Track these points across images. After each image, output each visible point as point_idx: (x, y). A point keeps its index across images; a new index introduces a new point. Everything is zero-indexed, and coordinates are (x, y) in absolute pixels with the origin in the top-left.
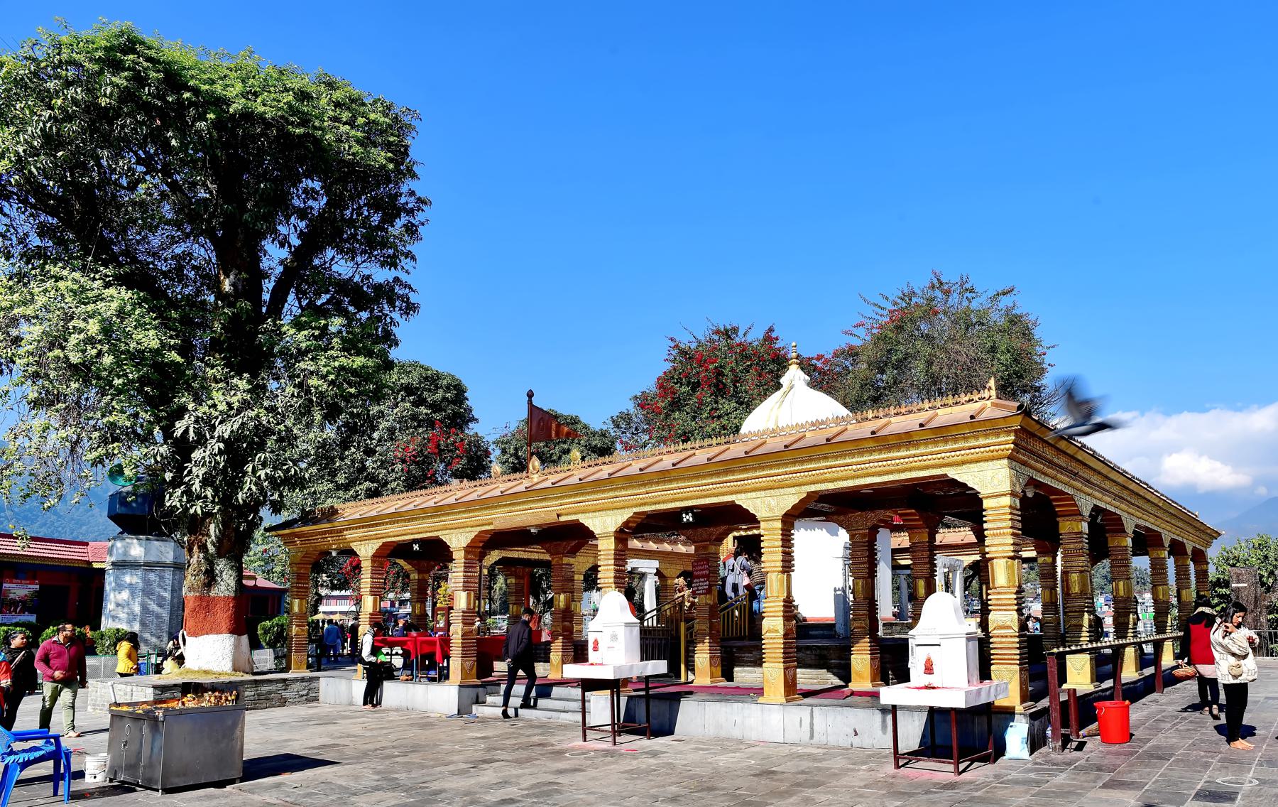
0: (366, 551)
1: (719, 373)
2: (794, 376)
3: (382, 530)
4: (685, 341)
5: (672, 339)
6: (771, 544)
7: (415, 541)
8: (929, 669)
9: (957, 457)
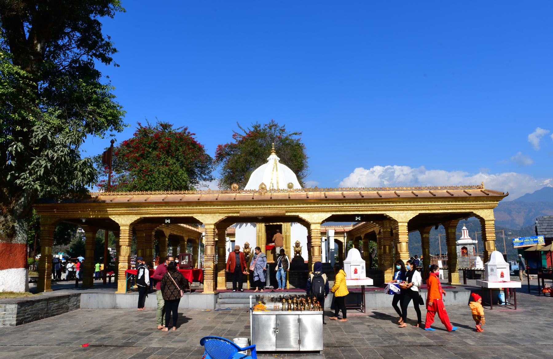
0: (124, 221)
1: (169, 145)
2: (273, 158)
3: (143, 210)
4: (144, 125)
5: (139, 124)
6: (403, 231)
8: (502, 276)
9: (478, 206)
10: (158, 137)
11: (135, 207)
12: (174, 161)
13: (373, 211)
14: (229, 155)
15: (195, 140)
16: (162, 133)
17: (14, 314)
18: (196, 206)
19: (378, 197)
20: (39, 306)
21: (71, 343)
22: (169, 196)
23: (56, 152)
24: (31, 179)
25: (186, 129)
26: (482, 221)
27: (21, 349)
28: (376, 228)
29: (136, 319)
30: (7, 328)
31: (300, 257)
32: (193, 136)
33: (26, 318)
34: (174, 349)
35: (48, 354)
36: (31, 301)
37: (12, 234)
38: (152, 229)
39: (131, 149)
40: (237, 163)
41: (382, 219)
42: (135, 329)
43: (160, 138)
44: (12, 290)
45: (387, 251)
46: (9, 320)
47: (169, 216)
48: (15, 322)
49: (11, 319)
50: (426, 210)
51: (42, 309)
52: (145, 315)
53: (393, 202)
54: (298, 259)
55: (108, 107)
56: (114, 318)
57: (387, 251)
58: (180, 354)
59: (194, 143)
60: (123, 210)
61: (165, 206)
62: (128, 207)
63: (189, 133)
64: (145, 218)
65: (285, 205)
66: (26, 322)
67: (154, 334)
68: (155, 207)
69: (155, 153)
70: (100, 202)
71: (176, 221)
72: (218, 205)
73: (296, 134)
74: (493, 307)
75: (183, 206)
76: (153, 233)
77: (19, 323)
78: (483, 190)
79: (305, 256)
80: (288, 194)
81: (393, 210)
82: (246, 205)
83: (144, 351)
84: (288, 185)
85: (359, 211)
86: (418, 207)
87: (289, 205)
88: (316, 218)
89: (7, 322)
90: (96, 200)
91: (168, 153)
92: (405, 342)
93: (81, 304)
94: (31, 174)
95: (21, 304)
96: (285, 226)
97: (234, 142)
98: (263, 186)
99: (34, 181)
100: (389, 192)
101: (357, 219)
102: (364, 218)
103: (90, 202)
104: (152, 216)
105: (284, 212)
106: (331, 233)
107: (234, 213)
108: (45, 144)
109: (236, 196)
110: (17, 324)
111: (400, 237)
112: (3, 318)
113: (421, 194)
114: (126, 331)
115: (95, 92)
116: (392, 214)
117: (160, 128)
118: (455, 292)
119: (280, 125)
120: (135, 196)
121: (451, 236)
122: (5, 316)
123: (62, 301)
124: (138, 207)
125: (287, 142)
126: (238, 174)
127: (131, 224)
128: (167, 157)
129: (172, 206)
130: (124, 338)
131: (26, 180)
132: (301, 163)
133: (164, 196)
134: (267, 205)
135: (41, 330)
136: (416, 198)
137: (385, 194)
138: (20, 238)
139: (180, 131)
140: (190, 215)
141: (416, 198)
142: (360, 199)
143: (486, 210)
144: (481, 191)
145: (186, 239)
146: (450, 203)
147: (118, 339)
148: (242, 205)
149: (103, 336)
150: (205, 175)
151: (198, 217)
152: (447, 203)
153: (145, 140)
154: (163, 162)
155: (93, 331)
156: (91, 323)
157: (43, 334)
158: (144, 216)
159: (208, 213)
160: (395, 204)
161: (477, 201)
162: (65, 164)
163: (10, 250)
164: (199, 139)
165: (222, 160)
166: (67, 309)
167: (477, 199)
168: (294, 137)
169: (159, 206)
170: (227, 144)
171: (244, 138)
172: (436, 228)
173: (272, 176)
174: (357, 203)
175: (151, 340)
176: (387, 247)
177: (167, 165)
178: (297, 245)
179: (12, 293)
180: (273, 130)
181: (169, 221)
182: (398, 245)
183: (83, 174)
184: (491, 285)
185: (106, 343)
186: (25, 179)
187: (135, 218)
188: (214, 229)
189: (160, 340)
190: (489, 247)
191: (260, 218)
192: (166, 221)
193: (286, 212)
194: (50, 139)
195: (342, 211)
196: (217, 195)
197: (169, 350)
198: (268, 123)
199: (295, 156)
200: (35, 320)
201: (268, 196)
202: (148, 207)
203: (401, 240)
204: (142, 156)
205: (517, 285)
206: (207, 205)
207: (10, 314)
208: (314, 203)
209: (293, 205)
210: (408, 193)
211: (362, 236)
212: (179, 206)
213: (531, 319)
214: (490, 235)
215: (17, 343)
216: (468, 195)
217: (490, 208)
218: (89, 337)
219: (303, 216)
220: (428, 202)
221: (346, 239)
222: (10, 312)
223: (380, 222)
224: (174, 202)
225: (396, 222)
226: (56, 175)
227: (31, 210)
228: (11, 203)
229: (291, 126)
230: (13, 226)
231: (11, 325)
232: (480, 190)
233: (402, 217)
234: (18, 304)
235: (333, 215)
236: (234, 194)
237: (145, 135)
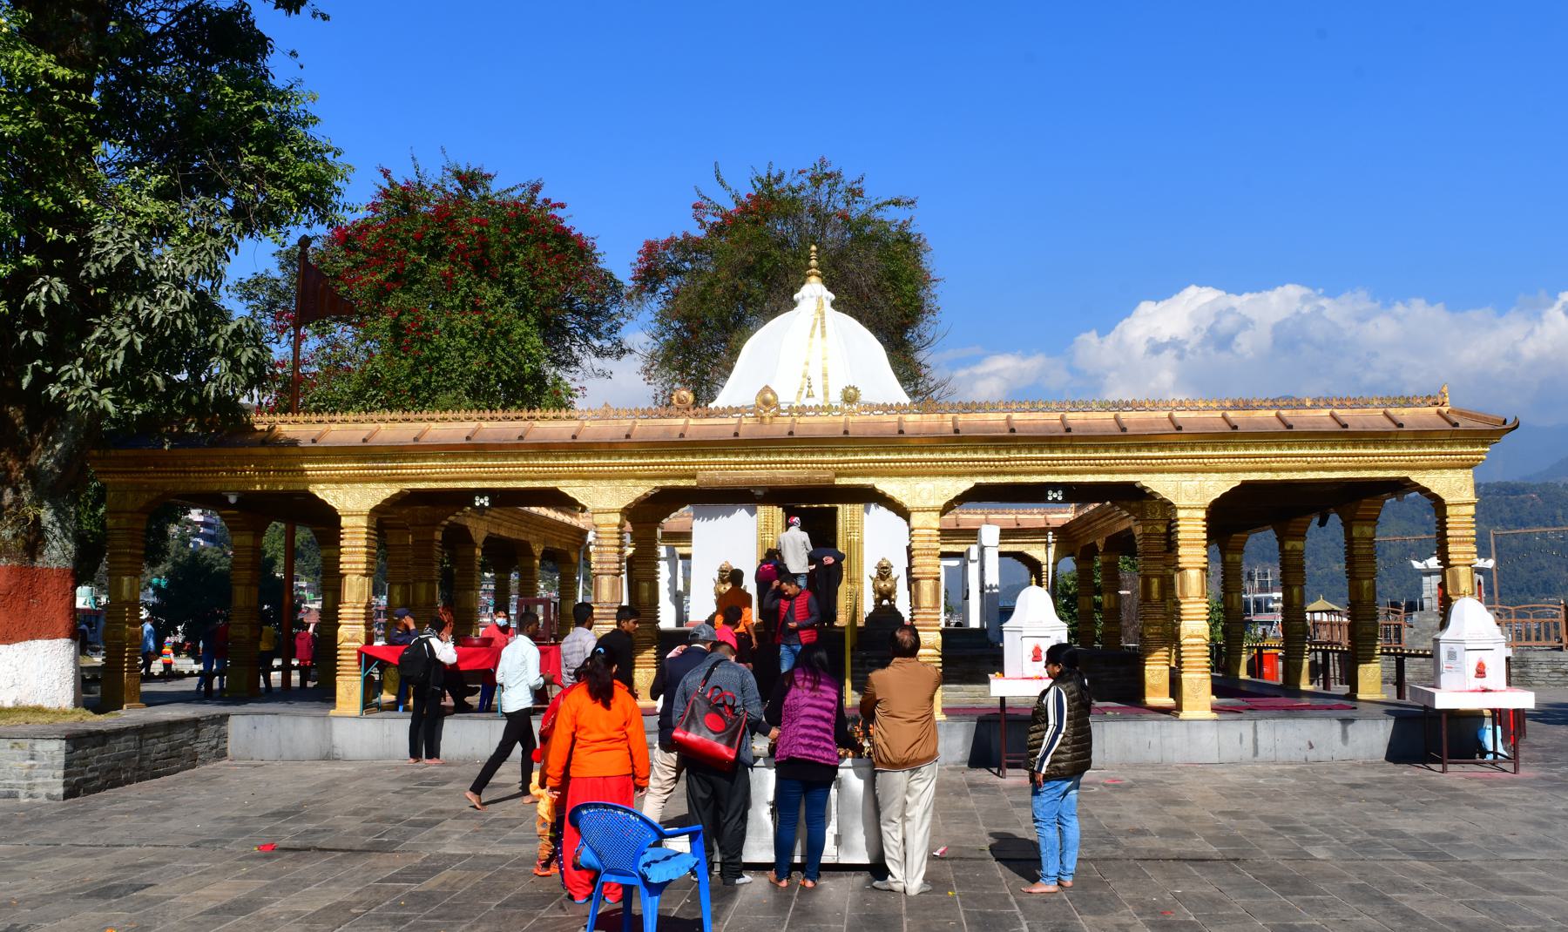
0: (354, 501)
2: (814, 293)
3: (410, 468)
5: (386, 174)
7: (482, 492)
8: (1481, 672)
10: (444, 217)
11: (384, 459)
12: (499, 292)
13: (1099, 472)
14: (677, 272)
15: (566, 225)
16: (460, 200)
17: (58, 767)
18: (567, 457)
19: (1116, 431)
20: (120, 746)
21: (228, 842)
22: (484, 424)
23: (158, 303)
24: (89, 383)
25: (536, 188)
26: (1438, 504)
27: (100, 853)
28: (1126, 522)
29: (397, 787)
30: (41, 805)
31: (892, 609)
32: (559, 212)
33: (87, 781)
34: (504, 859)
35: (177, 865)
36: (99, 733)
37: (34, 541)
38: (433, 523)
39: (361, 256)
40: (703, 300)
41: (1132, 495)
42: (394, 811)
43: (452, 221)
44: (39, 702)
45: (1155, 595)
46: (45, 784)
47: (486, 485)
48: (60, 791)
49: (50, 780)
50: (1263, 470)
51: (129, 757)
52: (419, 776)
53: (1162, 447)
54: (885, 615)
55: (299, 154)
56: (331, 785)
57: (1155, 595)
58: (522, 869)
59: (563, 235)
60: (348, 468)
61: (475, 457)
62: (365, 460)
63: (546, 201)
64: (416, 494)
65: (834, 453)
66: (89, 792)
67: (448, 824)
68: (445, 458)
69: (438, 269)
70: (282, 445)
71: (507, 499)
72: (631, 455)
73: (897, 203)
74: (1450, 767)
75: (526, 456)
76: (438, 536)
77: (71, 792)
78: (1445, 410)
79: (903, 605)
80: (842, 419)
81: (1162, 472)
82: (715, 454)
83: (424, 861)
84: (845, 391)
85: (1058, 473)
86: (1239, 463)
87: (845, 453)
88: (927, 492)
89: (38, 790)
90: (270, 440)
91: (482, 266)
92: (1137, 851)
93: (232, 746)
94: (87, 366)
95: (77, 741)
96: (845, 512)
97: (698, 233)
98: (769, 396)
99: (98, 390)
100: (1153, 415)
101: (1051, 495)
102: (1075, 493)
103: (253, 444)
104: (434, 485)
105: (829, 475)
106: (990, 535)
107: (681, 477)
108: (128, 279)
109: (686, 426)
110: (66, 796)
111: (1181, 551)
112: (28, 777)
113: (1249, 421)
114: (372, 815)
115: (260, 113)
116: (1159, 484)
117: (453, 186)
118: (1346, 721)
119: (849, 177)
120: (383, 425)
121: (1361, 549)
122: (34, 773)
123: (179, 737)
124: (393, 459)
125: (868, 230)
126: (701, 347)
127: (375, 511)
128: (480, 284)
129: (495, 457)
130: (367, 832)
131: (79, 387)
132: (917, 298)
133: (472, 425)
134: (780, 453)
135: (136, 812)
136: (1231, 436)
137: (1138, 423)
138: (57, 553)
139: (516, 194)
140: (550, 484)
141: (1231, 436)
142: (1061, 438)
143: (1449, 474)
144: (1439, 413)
145: (538, 549)
146: (1339, 451)
147: (351, 833)
148: (705, 453)
149: (311, 826)
150: (599, 337)
151: (572, 489)
152: (1327, 451)
153: (404, 225)
154: (462, 301)
155: (280, 814)
156: (270, 796)
157: (147, 820)
158: (411, 486)
159: (602, 478)
160: (1168, 454)
161: (1420, 446)
162: (185, 337)
163: (31, 587)
164: (577, 220)
165: (653, 290)
166: (193, 761)
167: (1422, 437)
168: (893, 215)
169: (455, 456)
170: (671, 240)
171: (726, 216)
172: (1322, 523)
173: (808, 358)
174: (1052, 448)
175: (440, 836)
176: (1155, 582)
177: (476, 308)
178: (884, 572)
179: (38, 710)
180: (824, 189)
181: (485, 501)
182: (1177, 576)
183: (235, 366)
184: (1444, 700)
185: (320, 843)
186: (73, 383)
187: (387, 491)
188: (621, 526)
189: (466, 838)
190: (1456, 585)
191: (760, 493)
192: (478, 502)
193: (837, 475)
194: (142, 265)
195: (1005, 473)
196: (628, 423)
197: (492, 860)
198: (808, 166)
199: (894, 277)
200: (112, 787)
201: (780, 426)
202: (425, 458)
203: (1183, 561)
204: (396, 277)
205: (1525, 700)
206: (598, 455)
207: (45, 767)
208: (921, 449)
209: (856, 453)
210: (1212, 418)
211: (1100, 543)
212: (516, 456)
213: (1541, 799)
214: (1461, 548)
215: (84, 840)
216: (1392, 427)
217: (1462, 467)
218: (272, 830)
219: (884, 485)
220: (1268, 447)
221: (1052, 550)
222: (47, 761)
223: (1134, 505)
224: (500, 446)
225: (1168, 507)
226: (158, 369)
227: (84, 469)
228: (29, 450)
229: (884, 170)
230: (37, 518)
231: (49, 797)
232: (1434, 410)
233: (1191, 491)
234: (67, 739)
235: (978, 486)
236: (681, 421)
237: (406, 208)
